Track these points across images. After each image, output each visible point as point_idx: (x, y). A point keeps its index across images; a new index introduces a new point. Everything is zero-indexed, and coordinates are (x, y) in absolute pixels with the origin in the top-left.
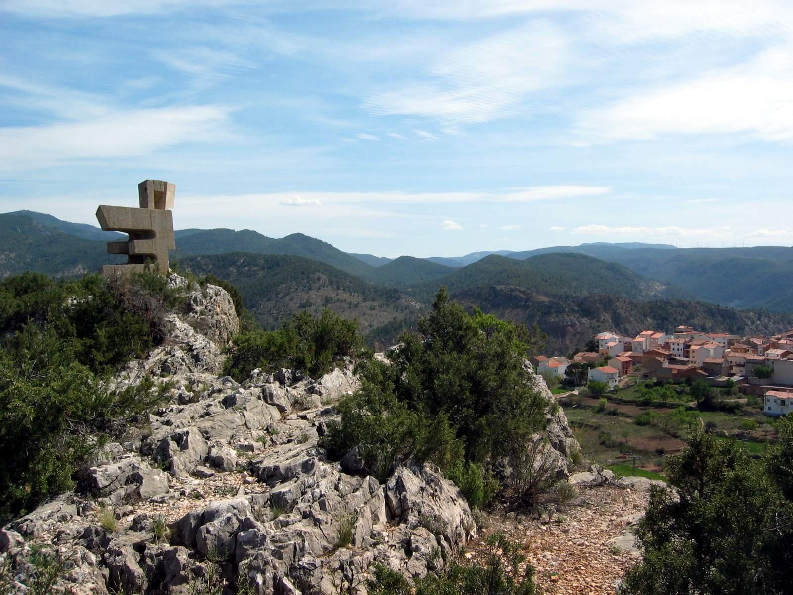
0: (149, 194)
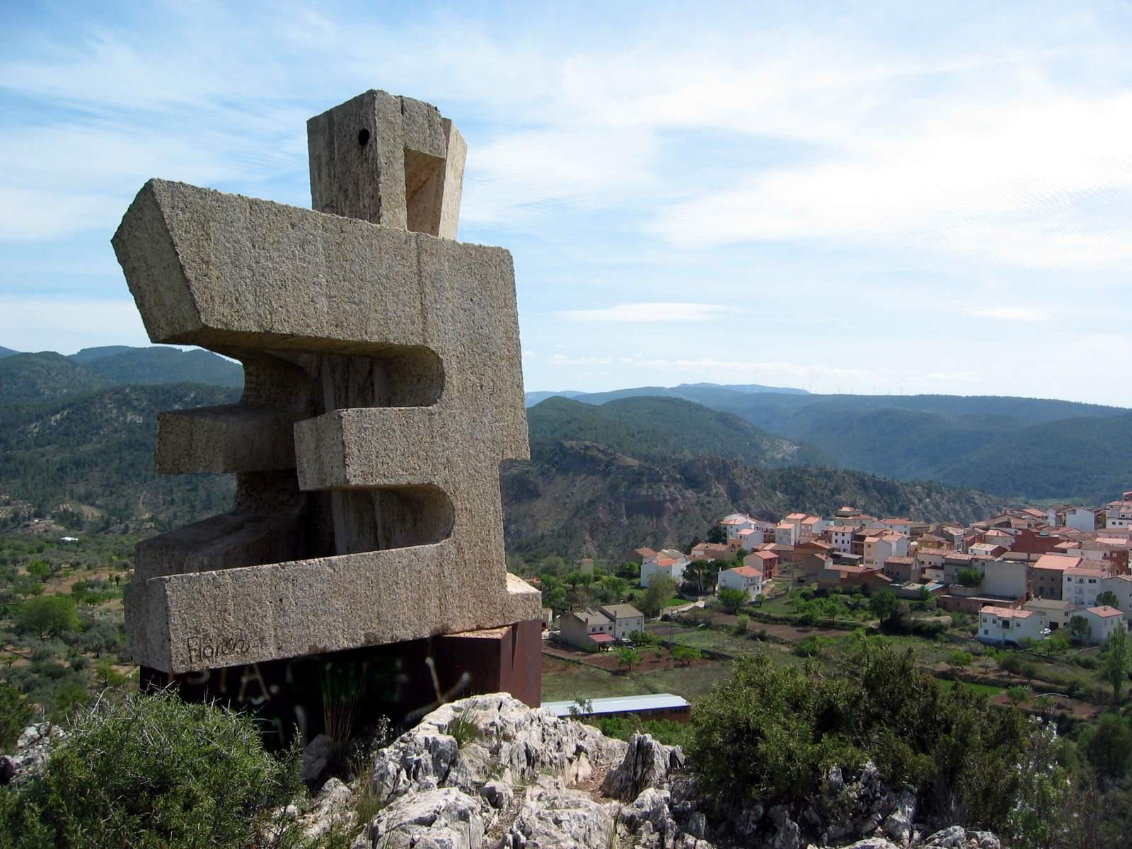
0: (382, 160)
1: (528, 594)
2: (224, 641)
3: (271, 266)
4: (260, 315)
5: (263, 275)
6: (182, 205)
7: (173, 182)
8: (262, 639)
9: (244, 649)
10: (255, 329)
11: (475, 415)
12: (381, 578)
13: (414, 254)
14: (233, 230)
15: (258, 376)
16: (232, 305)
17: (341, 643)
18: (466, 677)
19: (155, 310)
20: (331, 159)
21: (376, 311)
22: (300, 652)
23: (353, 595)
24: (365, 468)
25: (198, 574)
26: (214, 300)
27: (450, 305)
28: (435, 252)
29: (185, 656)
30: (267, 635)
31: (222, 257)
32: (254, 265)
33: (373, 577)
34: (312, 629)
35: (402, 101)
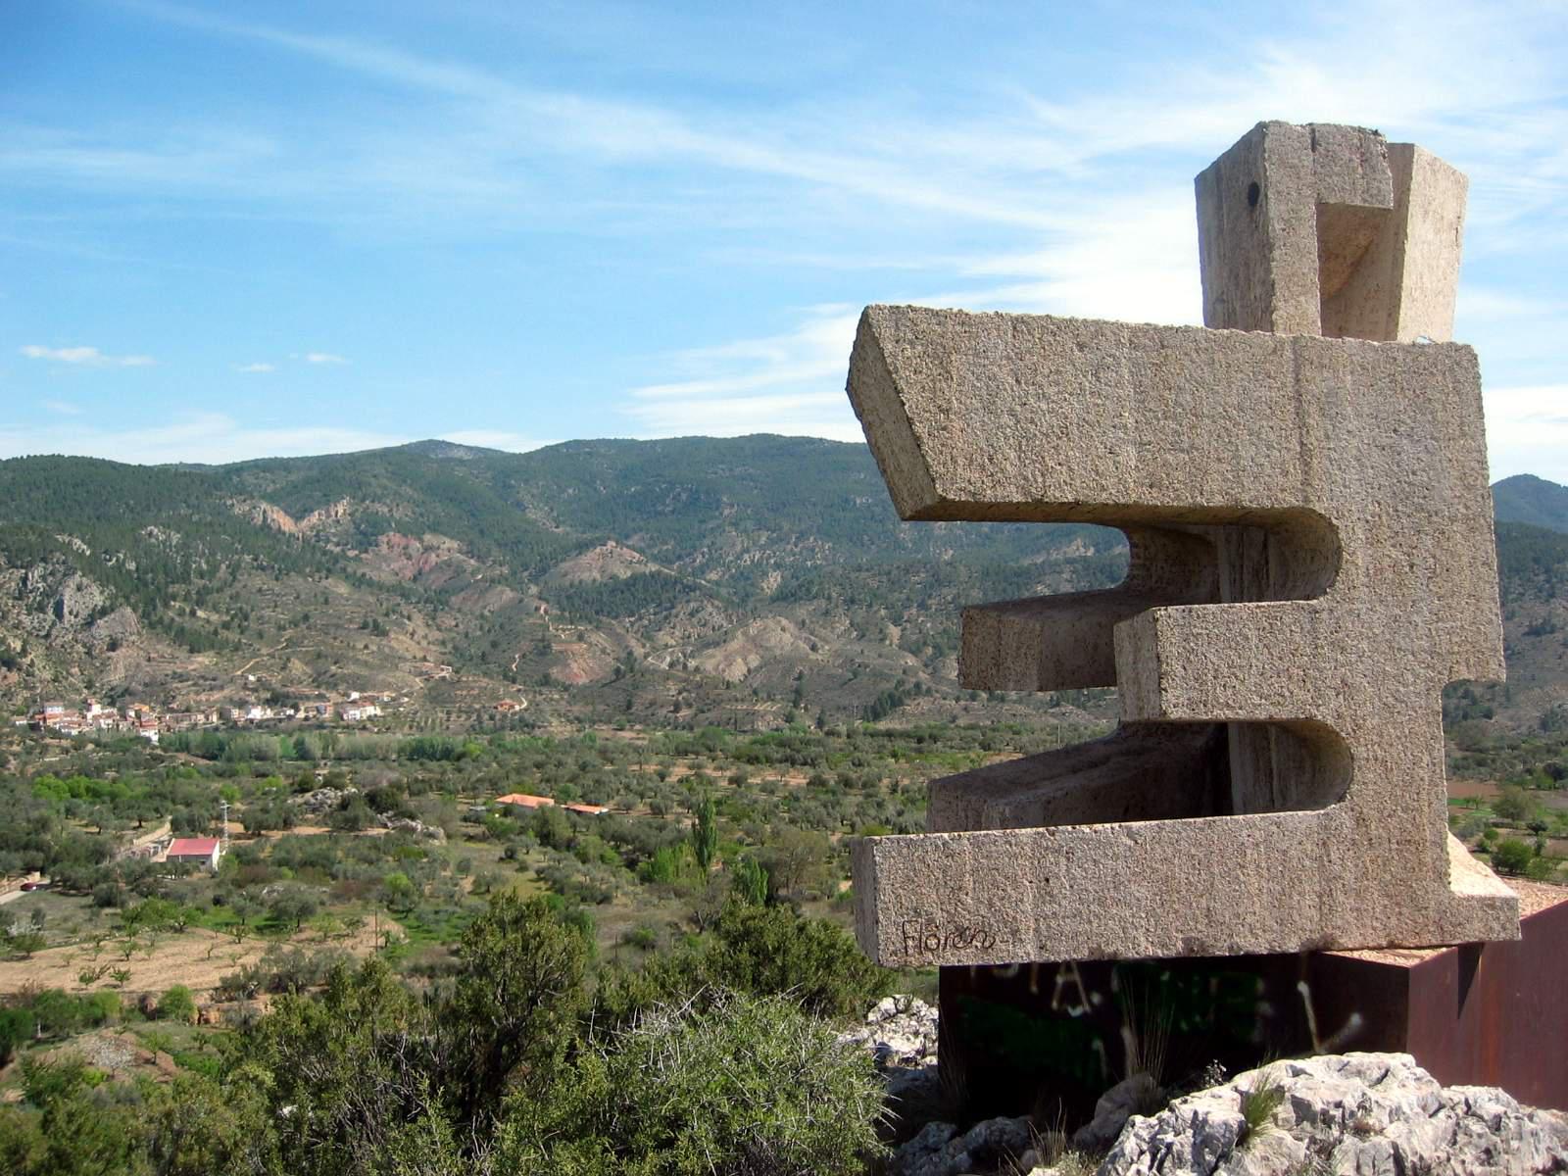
1: (1493, 899)
2: (957, 930)
3: (1044, 407)
4: (1026, 479)
5: (1032, 421)
6: (910, 336)
7: (897, 307)
8: (1015, 932)
9: (987, 944)
10: (1018, 498)
11: (1397, 611)
12: (1215, 858)
13: (1289, 367)
14: (986, 362)
15: (1146, 548)
16: (983, 468)
17: (1142, 949)
18: (1356, 1020)
19: (896, 477)
20: (1221, 230)
21: (1219, 460)
22: (1075, 956)
23: (1166, 880)
24: (1194, 694)
25: (922, 836)
26: (956, 462)
27: (1355, 442)
28: (1326, 361)
29: (898, 945)
30: (1022, 927)
31: (968, 401)
32: (1018, 408)
33: (1201, 855)
34: (1095, 925)
35: (1313, 131)
